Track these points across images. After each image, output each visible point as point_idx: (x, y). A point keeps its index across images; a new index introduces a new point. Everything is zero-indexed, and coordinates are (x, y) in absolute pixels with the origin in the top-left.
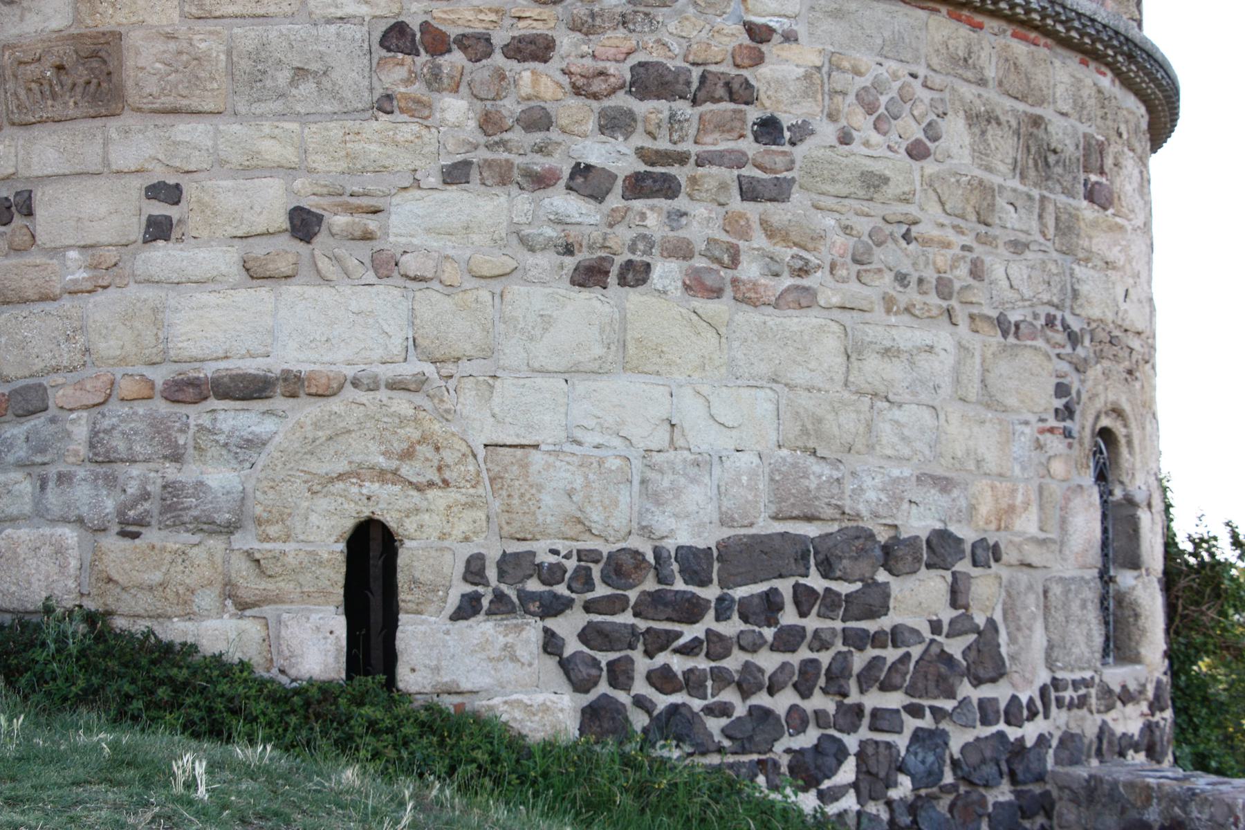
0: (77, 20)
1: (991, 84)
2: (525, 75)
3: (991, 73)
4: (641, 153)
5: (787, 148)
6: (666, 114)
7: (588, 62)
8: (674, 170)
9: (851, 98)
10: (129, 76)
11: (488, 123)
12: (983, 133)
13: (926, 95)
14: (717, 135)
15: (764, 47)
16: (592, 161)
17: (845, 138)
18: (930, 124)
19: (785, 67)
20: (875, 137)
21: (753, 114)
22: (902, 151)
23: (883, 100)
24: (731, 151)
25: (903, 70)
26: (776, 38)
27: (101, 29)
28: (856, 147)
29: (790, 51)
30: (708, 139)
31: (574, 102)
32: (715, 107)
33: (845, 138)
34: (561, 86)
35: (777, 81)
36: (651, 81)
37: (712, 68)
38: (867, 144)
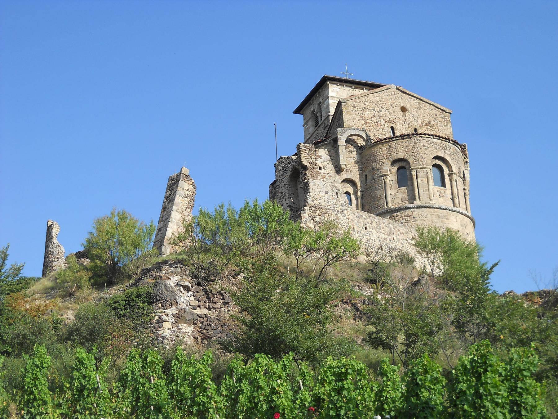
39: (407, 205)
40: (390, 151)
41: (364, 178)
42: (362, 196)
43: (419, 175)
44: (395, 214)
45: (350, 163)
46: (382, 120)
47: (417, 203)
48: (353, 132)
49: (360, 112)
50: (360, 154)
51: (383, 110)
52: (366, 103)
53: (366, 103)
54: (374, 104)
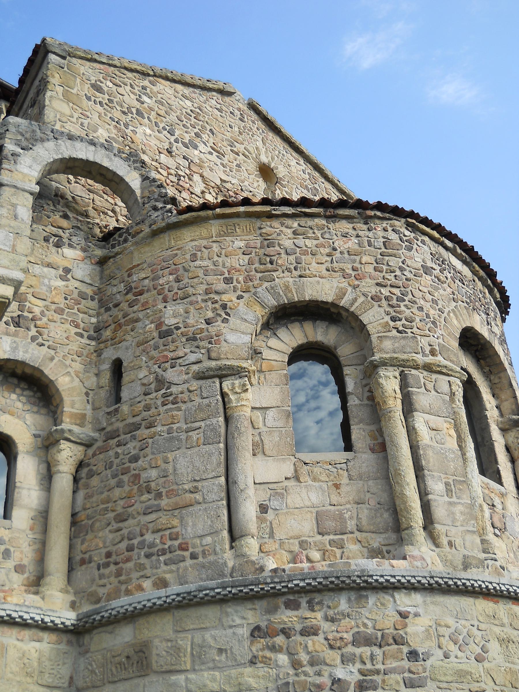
0: (135, 637)
1: (507, 625)
2: (310, 642)
3: (506, 621)
4: (361, 672)
5: (422, 663)
6: (369, 653)
7: (335, 634)
8: (375, 677)
9: (447, 638)
10: (154, 659)
11: (296, 664)
12: (507, 647)
13: (479, 633)
14: (392, 660)
15: (407, 620)
16: (340, 676)
17: (446, 656)
18: (483, 646)
19: (417, 628)
20: (460, 654)
21: (405, 649)
22: (473, 659)
23: (461, 637)
24: (399, 667)
25: (467, 624)
26: (411, 616)
27: (143, 640)
28: (452, 659)
29: (417, 620)
30: (388, 662)
31: (331, 652)
32: (389, 648)
33: (446, 656)
34: (323, 645)
35: (414, 634)
36: (362, 640)
37: (386, 631)
38: (456, 657)
39: (362, 563)
40: (267, 264)
41: (106, 378)
42: (81, 471)
43: (422, 399)
44: (287, 617)
45: (43, 290)
46: (196, 178)
47: (423, 558)
48: (83, 152)
49: (117, 114)
50: (102, 262)
51: (201, 147)
52: (145, 98)
53: (145, 98)
54: (173, 117)
